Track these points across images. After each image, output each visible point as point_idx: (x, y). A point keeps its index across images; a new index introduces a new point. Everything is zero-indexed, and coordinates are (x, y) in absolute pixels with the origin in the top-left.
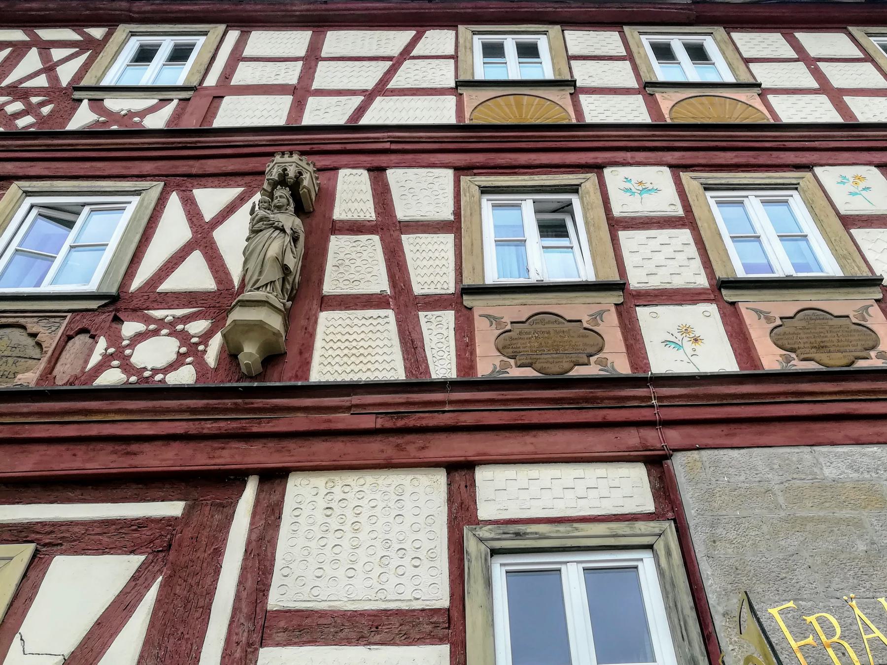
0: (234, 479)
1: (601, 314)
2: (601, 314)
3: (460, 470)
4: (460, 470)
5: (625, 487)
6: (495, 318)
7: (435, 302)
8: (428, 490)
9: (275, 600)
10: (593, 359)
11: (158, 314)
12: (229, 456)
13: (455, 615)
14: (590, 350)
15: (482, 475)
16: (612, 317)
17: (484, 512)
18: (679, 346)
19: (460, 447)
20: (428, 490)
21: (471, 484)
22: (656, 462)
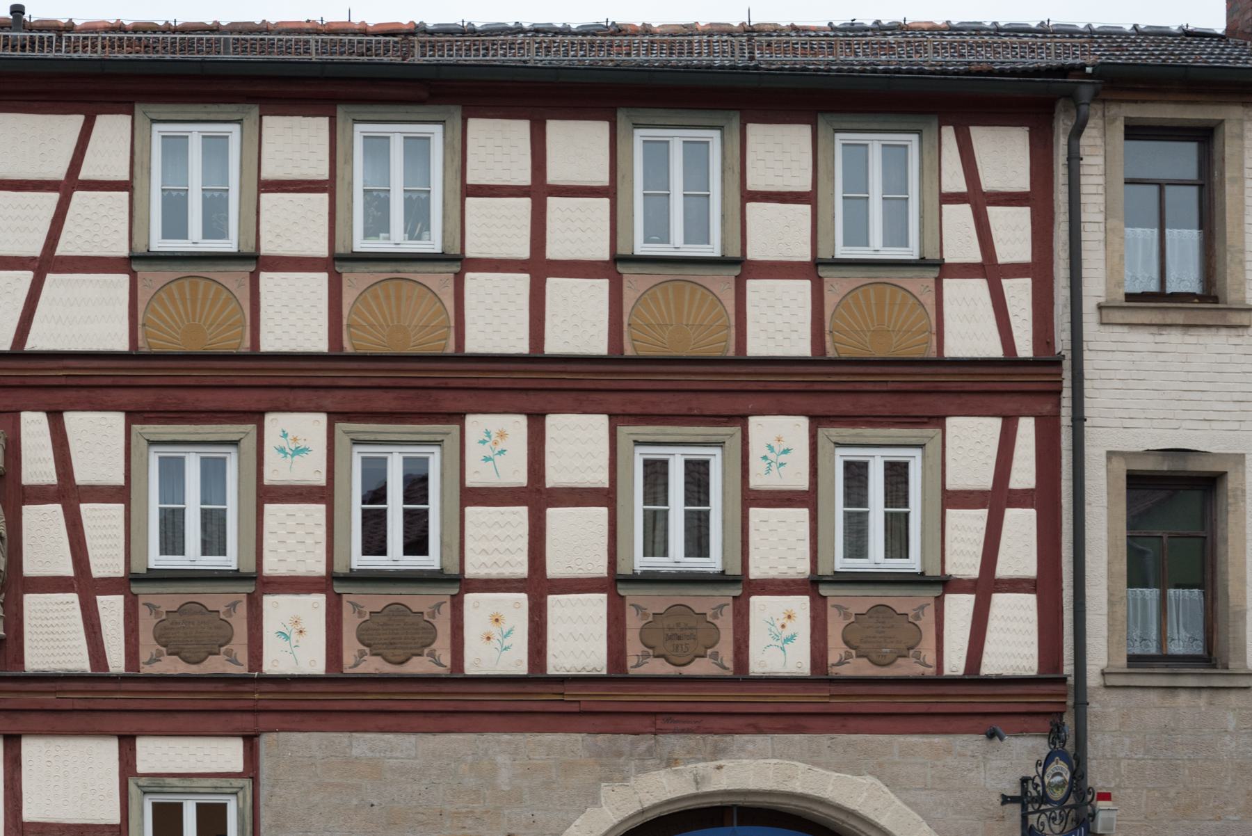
1: (234, 605)
2: (234, 605)
5: (226, 754)
6: (154, 607)
7: (110, 586)
8: (108, 750)
10: (223, 649)
13: (123, 828)
14: (222, 641)
16: (242, 610)
17: (141, 768)
18: (287, 638)
19: (128, 724)
21: (134, 749)
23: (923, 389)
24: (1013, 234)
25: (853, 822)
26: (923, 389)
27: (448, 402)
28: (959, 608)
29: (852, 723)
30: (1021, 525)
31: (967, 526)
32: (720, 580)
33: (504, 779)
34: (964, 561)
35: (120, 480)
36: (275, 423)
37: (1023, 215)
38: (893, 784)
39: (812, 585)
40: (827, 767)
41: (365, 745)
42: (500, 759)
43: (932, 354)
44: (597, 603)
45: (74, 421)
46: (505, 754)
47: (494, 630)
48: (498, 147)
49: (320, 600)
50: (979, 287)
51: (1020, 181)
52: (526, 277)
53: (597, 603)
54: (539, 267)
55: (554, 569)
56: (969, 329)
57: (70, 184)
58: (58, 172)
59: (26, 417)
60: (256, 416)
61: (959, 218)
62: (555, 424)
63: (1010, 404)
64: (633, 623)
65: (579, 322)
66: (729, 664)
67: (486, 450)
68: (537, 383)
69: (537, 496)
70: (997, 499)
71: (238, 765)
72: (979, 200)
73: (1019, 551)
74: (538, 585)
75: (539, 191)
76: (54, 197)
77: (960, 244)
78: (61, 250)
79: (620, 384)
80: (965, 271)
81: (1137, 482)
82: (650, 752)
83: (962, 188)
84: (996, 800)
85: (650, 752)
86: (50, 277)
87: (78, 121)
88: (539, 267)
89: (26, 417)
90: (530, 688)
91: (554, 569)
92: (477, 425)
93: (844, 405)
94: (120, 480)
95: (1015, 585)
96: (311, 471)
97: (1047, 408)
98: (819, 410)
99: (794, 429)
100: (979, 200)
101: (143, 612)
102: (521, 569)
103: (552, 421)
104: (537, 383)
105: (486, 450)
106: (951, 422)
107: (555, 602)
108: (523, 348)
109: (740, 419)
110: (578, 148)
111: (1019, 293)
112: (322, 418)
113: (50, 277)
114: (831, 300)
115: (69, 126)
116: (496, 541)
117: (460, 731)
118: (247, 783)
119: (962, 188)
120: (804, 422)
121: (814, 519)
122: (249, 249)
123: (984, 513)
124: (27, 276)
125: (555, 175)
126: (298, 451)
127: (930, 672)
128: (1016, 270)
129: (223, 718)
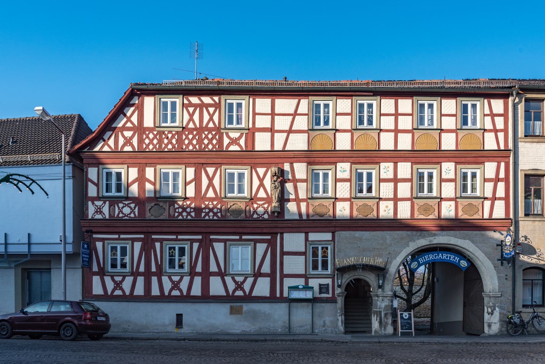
0: (277, 233)
3: (307, 234)
4: (307, 234)
5: (328, 236)
7: (303, 200)
8: (303, 235)
9: (285, 250)
11: (259, 202)
12: (275, 231)
15: (309, 234)
17: (310, 239)
19: (307, 230)
20: (303, 235)
22: (333, 233)
23: (479, 156)
24: (500, 123)
25: (464, 250)
26: (479, 156)
27: (377, 160)
28: (487, 204)
29: (464, 228)
30: (501, 186)
31: (489, 186)
32: (435, 198)
33: (388, 241)
34: (488, 194)
35: (306, 178)
36: (339, 165)
37: (502, 118)
38: (473, 242)
39: (455, 199)
40: (459, 238)
41: (358, 234)
42: (388, 237)
43: (482, 149)
44: (409, 203)
45: (295, 165)
46: (388, 236)
47: (386, 209)
48: (388, 104)
49: (348, 203)
50: (493, 134)
51: (502, 111)
52: (393, 133)
53: (409, 203)
54: (397, 131)
55: (399, 196)
56: (490, 143)
57: (295, 114)
58: (292, 111)
59: (285, 164)
60: (335, 163)
61: (488, 119)
62: (399, 164)
63: (499, 159)
64: (416, 207)
65: (405, 143)
66: (437, 216)
67: (385, 170)
68: (396, 156)
69: (396, 180)
70: (497, 180)
71: (331, 239)
72: (493, 115)
73: (501, 192)
74: (396, 200)
75: (396, 115)
76: (291, 117)
77: (488, 125)
78: (293, 129)
79: (415, 156)
80: (490, 131)
81: (526, 175)
82: (420, 235)
83: (489, 113)
84: (495, 245)
85: (420, 235)
86: (291, 134)
87: (296, 101)
88: (397, 131)
89: (285, 164)
90: (394, 221)
91: (399, 196)
92: (383, 165)
93: (463, 160)
94: (306, 178)
95: (500, 199)
96: (346, 175)
97: (507, 160)
98: (457, 161)
99: (451, 165)
100: (493, 115)
101: (310, 205)
102: (392, 196)
103: (399, 164)
104: (396, 156)
105: (385, 170)
106: (486, 163)
107: (399, 203)
108: (393, 148)
109: (439, 163)
110: (405, 105)
111: (501, 135)
112: (349, 164)
113: (291, 134)
114: (460, 137)
115: (294, 101)
116: (387, 190)
117: (379, 231)
118: (333, 242)
119: (489, 113)
120: (453, 164)
121: (456, 185)
122: (334, 128)
123: (493, 183)
124: (286, 134)
125: (400, 111)
126: (344, 171)
127: (481, 218)
128: (501, 131)
129: (328, 228)
